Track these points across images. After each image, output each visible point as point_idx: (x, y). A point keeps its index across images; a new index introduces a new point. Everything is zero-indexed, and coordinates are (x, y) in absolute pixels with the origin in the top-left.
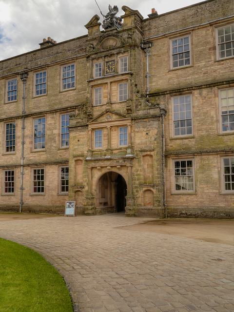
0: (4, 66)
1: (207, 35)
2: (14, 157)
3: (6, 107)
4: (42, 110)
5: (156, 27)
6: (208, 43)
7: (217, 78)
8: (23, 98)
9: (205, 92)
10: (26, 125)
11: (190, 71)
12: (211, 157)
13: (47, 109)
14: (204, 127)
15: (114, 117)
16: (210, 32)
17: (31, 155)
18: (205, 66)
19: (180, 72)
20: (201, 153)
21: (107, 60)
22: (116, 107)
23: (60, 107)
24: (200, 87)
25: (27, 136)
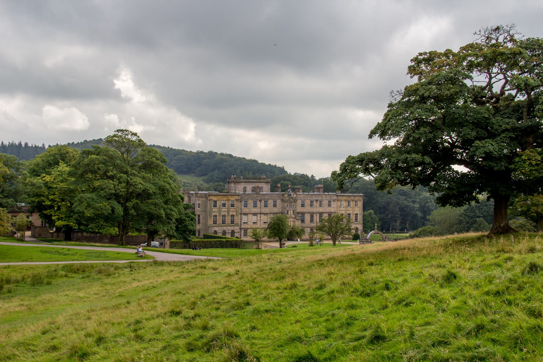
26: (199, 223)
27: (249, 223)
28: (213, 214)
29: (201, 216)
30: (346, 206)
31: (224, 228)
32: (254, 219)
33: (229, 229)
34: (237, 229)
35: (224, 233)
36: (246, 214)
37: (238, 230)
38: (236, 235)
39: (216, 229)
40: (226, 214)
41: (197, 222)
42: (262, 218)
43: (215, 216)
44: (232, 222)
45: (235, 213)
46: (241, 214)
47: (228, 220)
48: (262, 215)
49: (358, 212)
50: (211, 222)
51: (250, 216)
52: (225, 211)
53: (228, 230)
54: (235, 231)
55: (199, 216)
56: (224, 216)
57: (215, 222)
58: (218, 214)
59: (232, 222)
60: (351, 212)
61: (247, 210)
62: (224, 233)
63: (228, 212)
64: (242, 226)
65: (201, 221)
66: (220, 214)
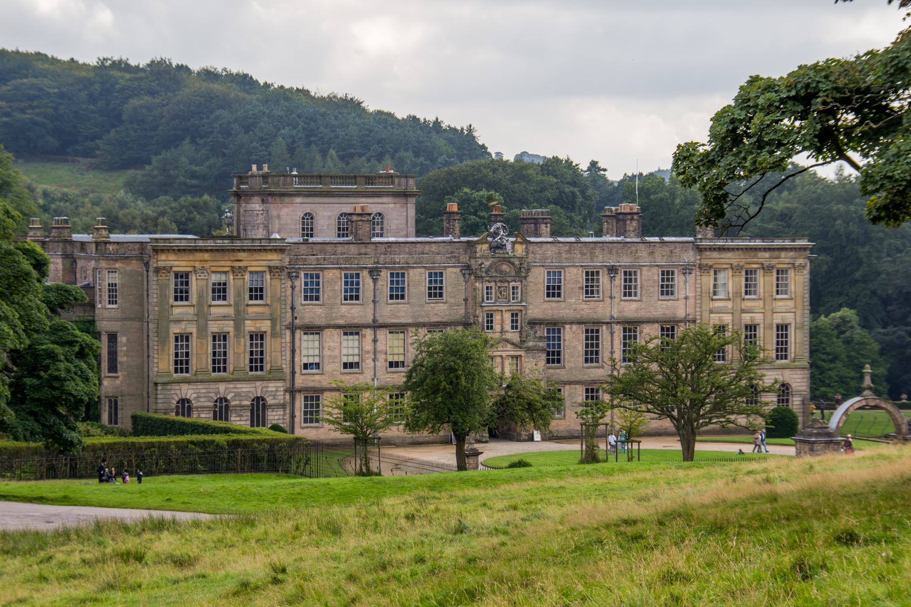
0: (339, 252)
1: (577, 274)
2: (361, 377)
3: (344, 309)
4: (402, 321)
5: (533, 253)
6: (578, 282)
7: (585, 317)
8: (374, 301)
9: (574, 327)
10: (378, 336)
11: (563, 305)
12: (577, 386)
13: (410, 321)
14: (573, 359)
15: (509, 347)
16: (580, 272)
17: (388, 375)
18: (575, 303)
19: (554, 304)
20: (570, 383)
21: (499, 284)
22: (509, 336)
23: (426, 320)
24: (571, 323)
25: (381, 352)
26: (113, 368)
27: (328, 367)
28: (175, 329)
29: (122, 339)
30: (737, 294)
31: (222, 387)
32: (348, 348)
33: (241, 392)
34: (274, 392)
35: (222, 408)
36: (313, 329)
37: (282, 397)
38: (274, 416)
39: (188, 392)
40: (229, 327)
41: (105, 365)
42: (380, 346)
43: (186, 337)
44: (257, 362)
45: (265, 326)
46: (293, 328)
47: (238, 353)
48: (382, 334)
49: (789, 318)
50: (163, 363)
51: (332, 338)
52: (225, 318)
53: (237, 395)
54: (270, 401)
55: (113, 338)
56: (221, 338)
57: (182, 364)
58: (192, 329)
59: (257, 362)
60: (758, 318)
61: (319, 310)
62: (222, 408)
63: (239, 320)
64: (300, 381)
65: (121, 359)
66: (202, 330)
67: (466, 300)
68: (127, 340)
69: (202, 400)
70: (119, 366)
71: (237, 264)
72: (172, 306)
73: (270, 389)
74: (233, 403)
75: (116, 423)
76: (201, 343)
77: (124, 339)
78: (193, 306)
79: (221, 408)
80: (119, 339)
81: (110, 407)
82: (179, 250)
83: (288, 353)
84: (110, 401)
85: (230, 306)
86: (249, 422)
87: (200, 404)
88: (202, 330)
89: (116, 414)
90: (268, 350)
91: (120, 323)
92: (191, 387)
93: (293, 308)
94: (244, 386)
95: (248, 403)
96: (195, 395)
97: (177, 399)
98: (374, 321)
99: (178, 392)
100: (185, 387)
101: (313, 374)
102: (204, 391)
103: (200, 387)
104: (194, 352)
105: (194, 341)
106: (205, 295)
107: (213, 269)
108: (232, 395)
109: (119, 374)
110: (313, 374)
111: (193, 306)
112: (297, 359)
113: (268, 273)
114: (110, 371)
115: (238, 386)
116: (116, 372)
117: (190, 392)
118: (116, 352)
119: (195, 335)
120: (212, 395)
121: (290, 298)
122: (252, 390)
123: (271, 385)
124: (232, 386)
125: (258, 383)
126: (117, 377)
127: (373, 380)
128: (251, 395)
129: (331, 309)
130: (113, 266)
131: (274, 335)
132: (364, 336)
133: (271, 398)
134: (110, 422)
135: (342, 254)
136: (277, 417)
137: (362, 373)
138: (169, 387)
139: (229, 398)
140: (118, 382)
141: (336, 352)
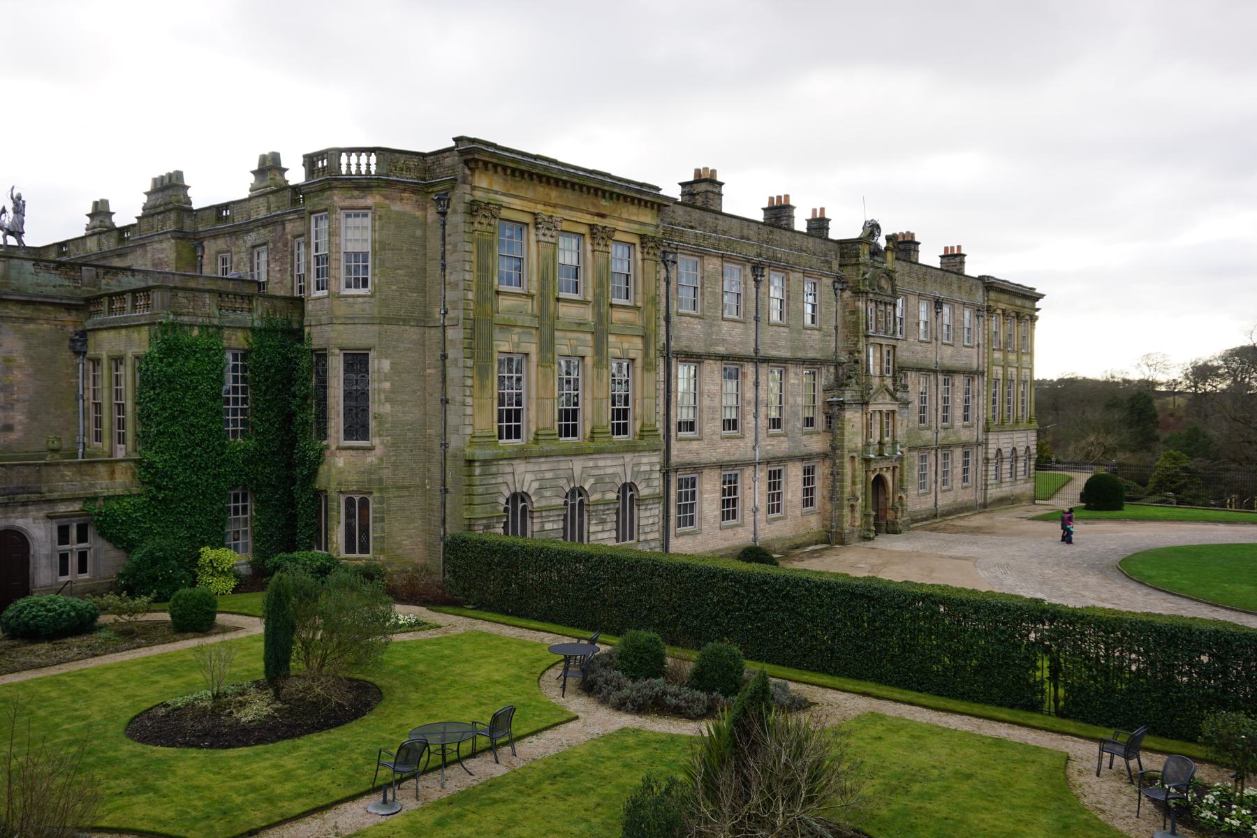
26: (357, 427)
29: (379, 365)
31: (578, 465)
32: (721, 392)
35: (576, 505)
39: (524, 476)
43: (514, 362)
50: (476, 417)
52: (580, 325)
53: (599, 480)
55: (357, 362)
57: (510, 421)
62: (576, 505)
65: (378, 407)
66: (547, 346)
67: (836, 328)
68: (393, 365)
69: (548, 494)
70: (372, 424)
71: (600, 222)
72: (498, 292)
73: (643, 468)
74: (594, 497)
75: (365, 549)
76: (545, 375)
77: (386, 365)
78: (529, 296)
79: (573, 506)
80: (373, 364)
81: (350, 515)
82: (514, 170)
83: (661, 401)
84: (350, 503)
85: (585, 302)
86: (614, 534)
87: (544, 503)
88: (547, 346)
89: (365, 530)
90: (638, 395)
91: (376, 328)
92: (530, 467)
93: (668, 319)
94: (609, 462)
95: (612, 496)
96: (536, 485)
97: (507, 494)
98: (756, 351)
99: (509, 478)
100: (521, 467)
101: (691, 440)
102: (549, 475)
103: (544, 467)
104: (533, 394)
105: (532, 371)
106: (551, 278)
107: (565, 226)
108: (592, 481)
109: (376, 441)
110: (691, 440)
111: (529, 296)
112: (673, 413)
113: (638, 248)
114: (349, 434)
115: (601, 463)
116: (366, 438)
117: (529, 477)
118: (365, 394)
119: (534, 358)
120: (563, 482)
121: (664, 300)
122: (620, 470)
123: (645, 460)
124: (591, 464)
125: (628, 457)
126: (372, 449)
127: (754, 448)
128: (617, 480)
129: (711, 326)
130: (362, 202)
131: (648, 366)
132: (744, 375)
133: (644, 484)
134: (350, 548)
135: (724, 232)
136: (651, 521)
137: (742, 437)
138: (494, 469)
139: (586, 488)
140: (371, 459)
141: (716, 402)
